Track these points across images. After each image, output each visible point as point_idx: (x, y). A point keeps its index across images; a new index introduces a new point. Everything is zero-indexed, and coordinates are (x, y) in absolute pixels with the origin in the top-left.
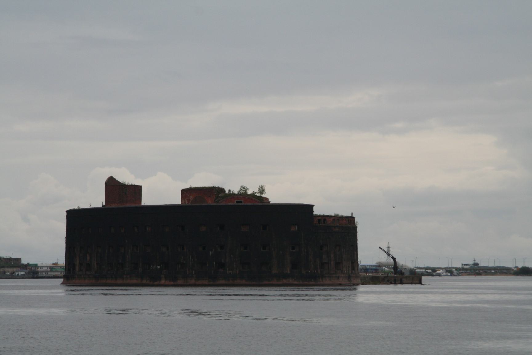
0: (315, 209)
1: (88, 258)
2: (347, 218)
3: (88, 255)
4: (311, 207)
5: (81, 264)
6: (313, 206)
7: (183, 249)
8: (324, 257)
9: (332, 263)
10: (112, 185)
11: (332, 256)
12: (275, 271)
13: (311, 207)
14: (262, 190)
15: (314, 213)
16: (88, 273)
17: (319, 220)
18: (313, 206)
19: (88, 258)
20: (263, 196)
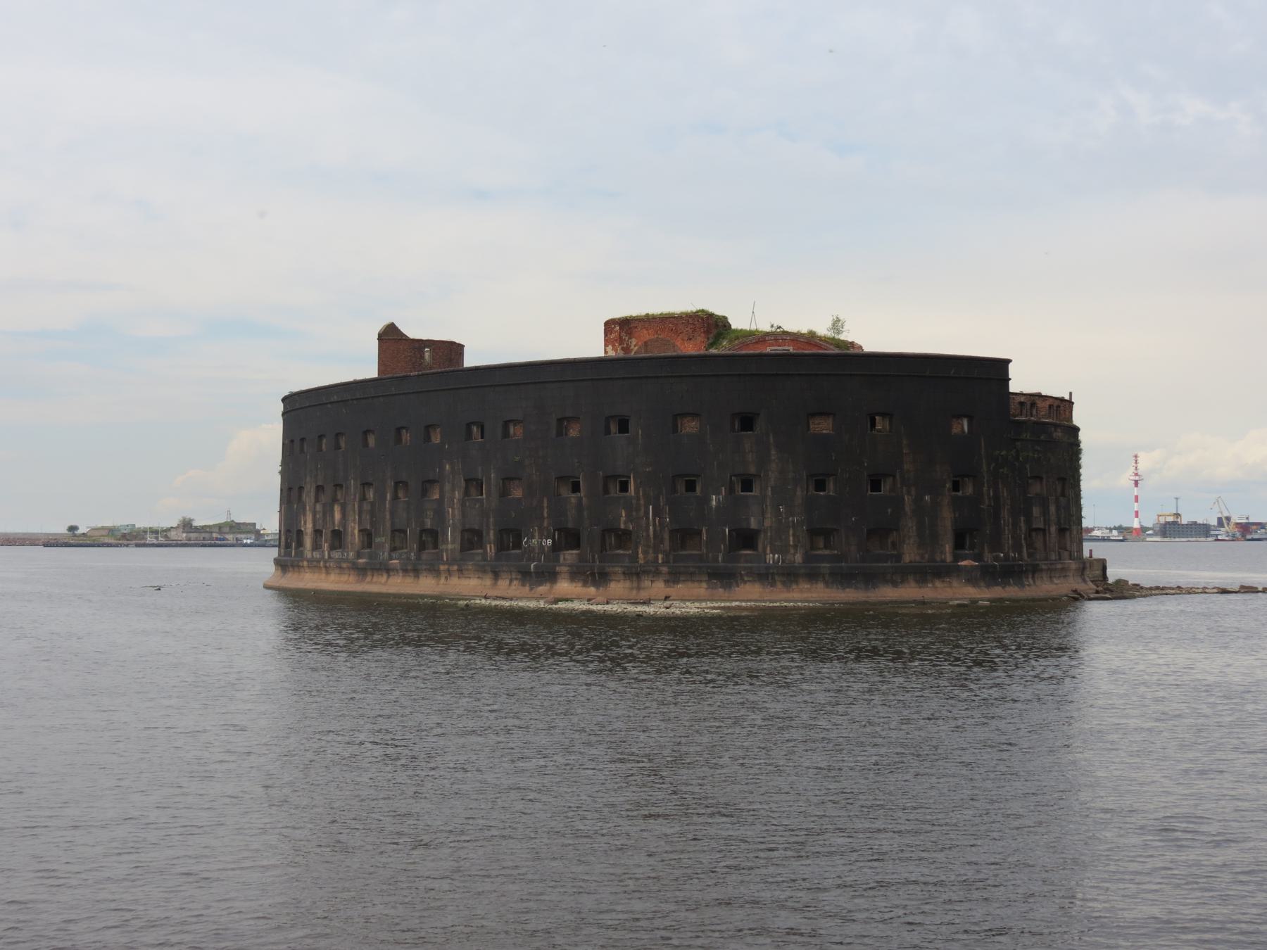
0: (1013, 370)
1: (337, 516)
2: (1062, 400)
3: (337, 509)
4: (999, 368)
5: (317, 532)
6: (1009, 361)
7: (624, 487)
8: (1036, 511)
9: (1053, 529)
10: (390, 337)
11: (1052, 509)
12: (910, 554)
13: (999, 368)
14: (837, 324)
15: (1014, 387)
16: (336, 554)
17: (1022, 404)
18: (1008, 361)
19: (337, 516)
20: (842, 337)
